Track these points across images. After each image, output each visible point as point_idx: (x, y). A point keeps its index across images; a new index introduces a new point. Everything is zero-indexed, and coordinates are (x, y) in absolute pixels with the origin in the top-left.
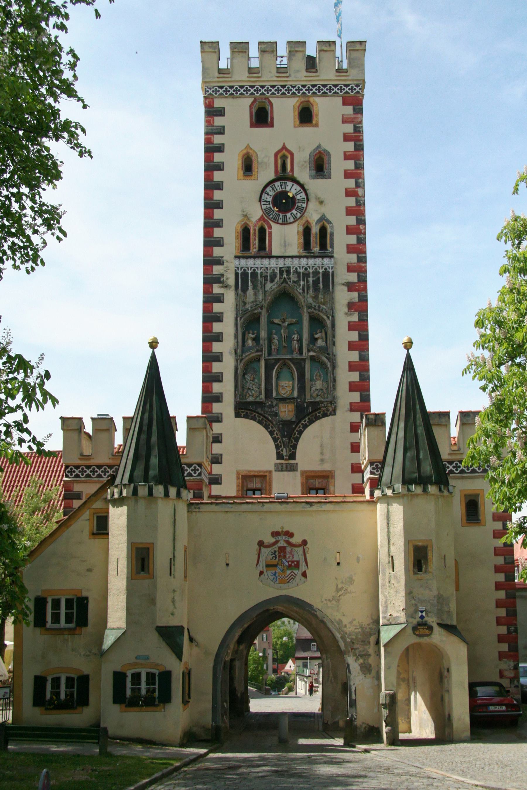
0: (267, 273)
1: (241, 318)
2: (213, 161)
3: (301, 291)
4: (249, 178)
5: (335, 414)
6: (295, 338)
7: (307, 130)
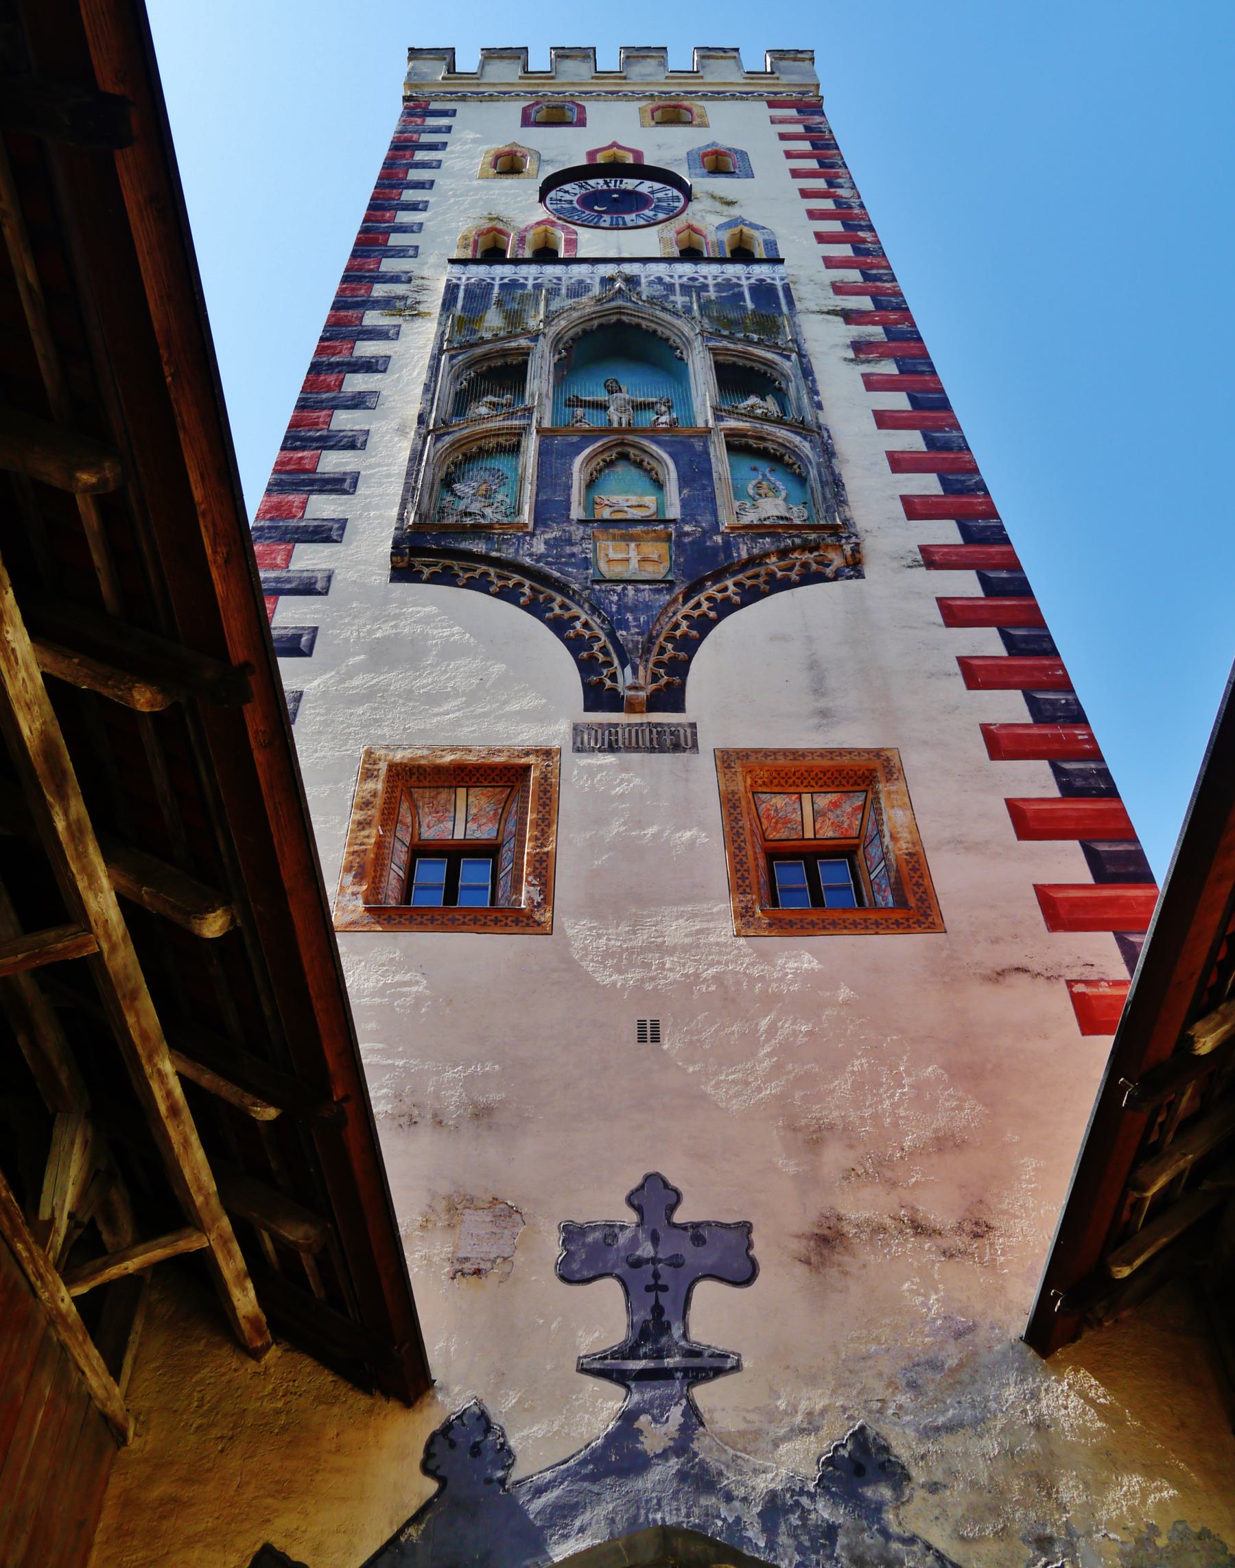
1: (452, 358)
5: (860, 575)
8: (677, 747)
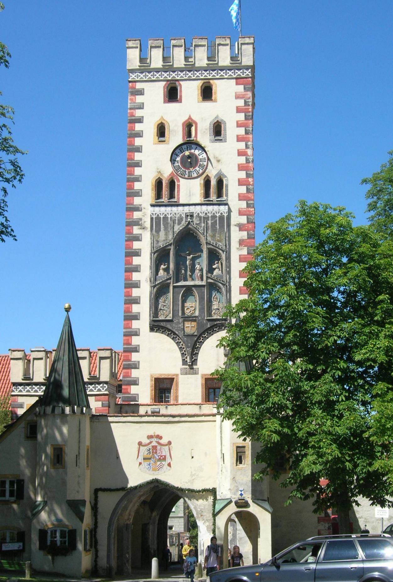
1: (154, 254)
2: (134, 130)
7: (208, 105)
8: (196, 374)
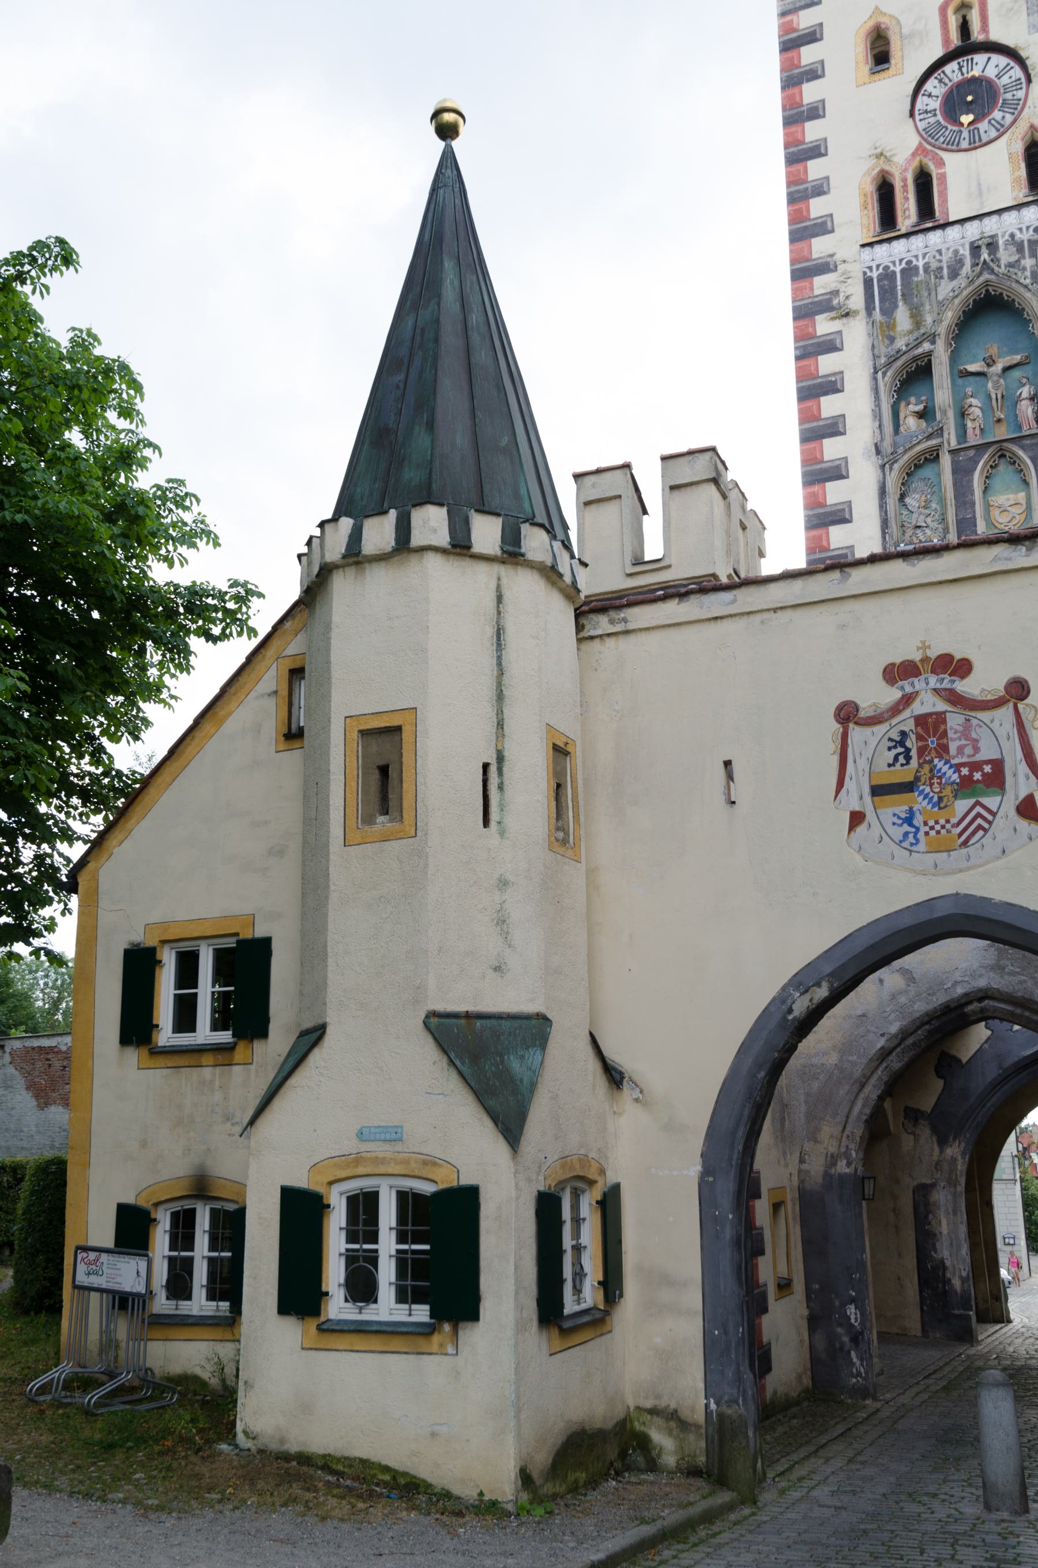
0: (940, 261)
1: (884, 374)
2: (798, 66)
3: (1028, 281)
4: (883, 75)
6: (1025, 394)
